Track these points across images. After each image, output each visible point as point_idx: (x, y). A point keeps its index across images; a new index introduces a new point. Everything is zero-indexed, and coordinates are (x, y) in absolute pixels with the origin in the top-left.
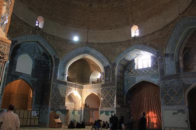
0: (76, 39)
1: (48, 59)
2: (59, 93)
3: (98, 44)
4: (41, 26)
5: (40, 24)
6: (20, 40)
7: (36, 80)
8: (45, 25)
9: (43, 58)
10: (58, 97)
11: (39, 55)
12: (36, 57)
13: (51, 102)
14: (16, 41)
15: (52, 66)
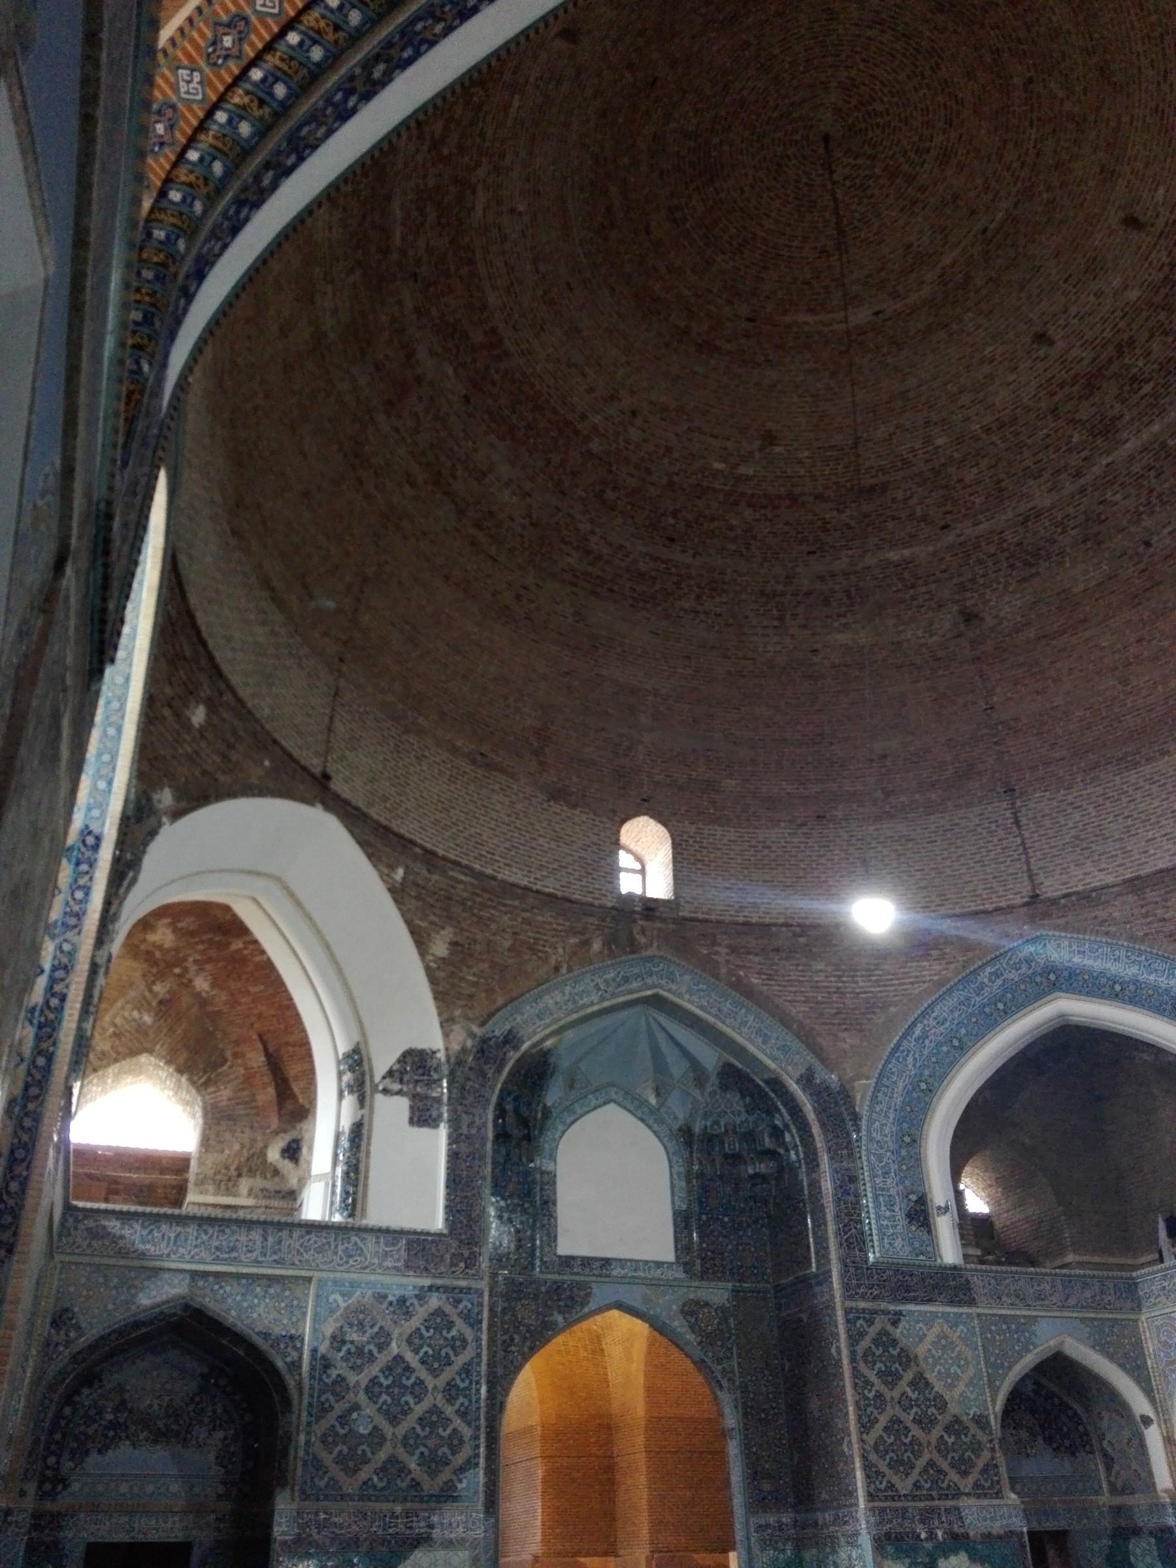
0: (873, 915)
1: (771, 1111)
2: (920, 1382)
3: (1135, 885)
4: (658, 882)
5: (646, 861)
6: (539, 1021)
7: (718, 1294)
8: (684, 860)
9: (734, 1110)
10: (926, 1423)
11: (696, 1093)
12: (678, 1110)
13: (867, 1466)
14: (511, 1039)
15: (813, 1162)
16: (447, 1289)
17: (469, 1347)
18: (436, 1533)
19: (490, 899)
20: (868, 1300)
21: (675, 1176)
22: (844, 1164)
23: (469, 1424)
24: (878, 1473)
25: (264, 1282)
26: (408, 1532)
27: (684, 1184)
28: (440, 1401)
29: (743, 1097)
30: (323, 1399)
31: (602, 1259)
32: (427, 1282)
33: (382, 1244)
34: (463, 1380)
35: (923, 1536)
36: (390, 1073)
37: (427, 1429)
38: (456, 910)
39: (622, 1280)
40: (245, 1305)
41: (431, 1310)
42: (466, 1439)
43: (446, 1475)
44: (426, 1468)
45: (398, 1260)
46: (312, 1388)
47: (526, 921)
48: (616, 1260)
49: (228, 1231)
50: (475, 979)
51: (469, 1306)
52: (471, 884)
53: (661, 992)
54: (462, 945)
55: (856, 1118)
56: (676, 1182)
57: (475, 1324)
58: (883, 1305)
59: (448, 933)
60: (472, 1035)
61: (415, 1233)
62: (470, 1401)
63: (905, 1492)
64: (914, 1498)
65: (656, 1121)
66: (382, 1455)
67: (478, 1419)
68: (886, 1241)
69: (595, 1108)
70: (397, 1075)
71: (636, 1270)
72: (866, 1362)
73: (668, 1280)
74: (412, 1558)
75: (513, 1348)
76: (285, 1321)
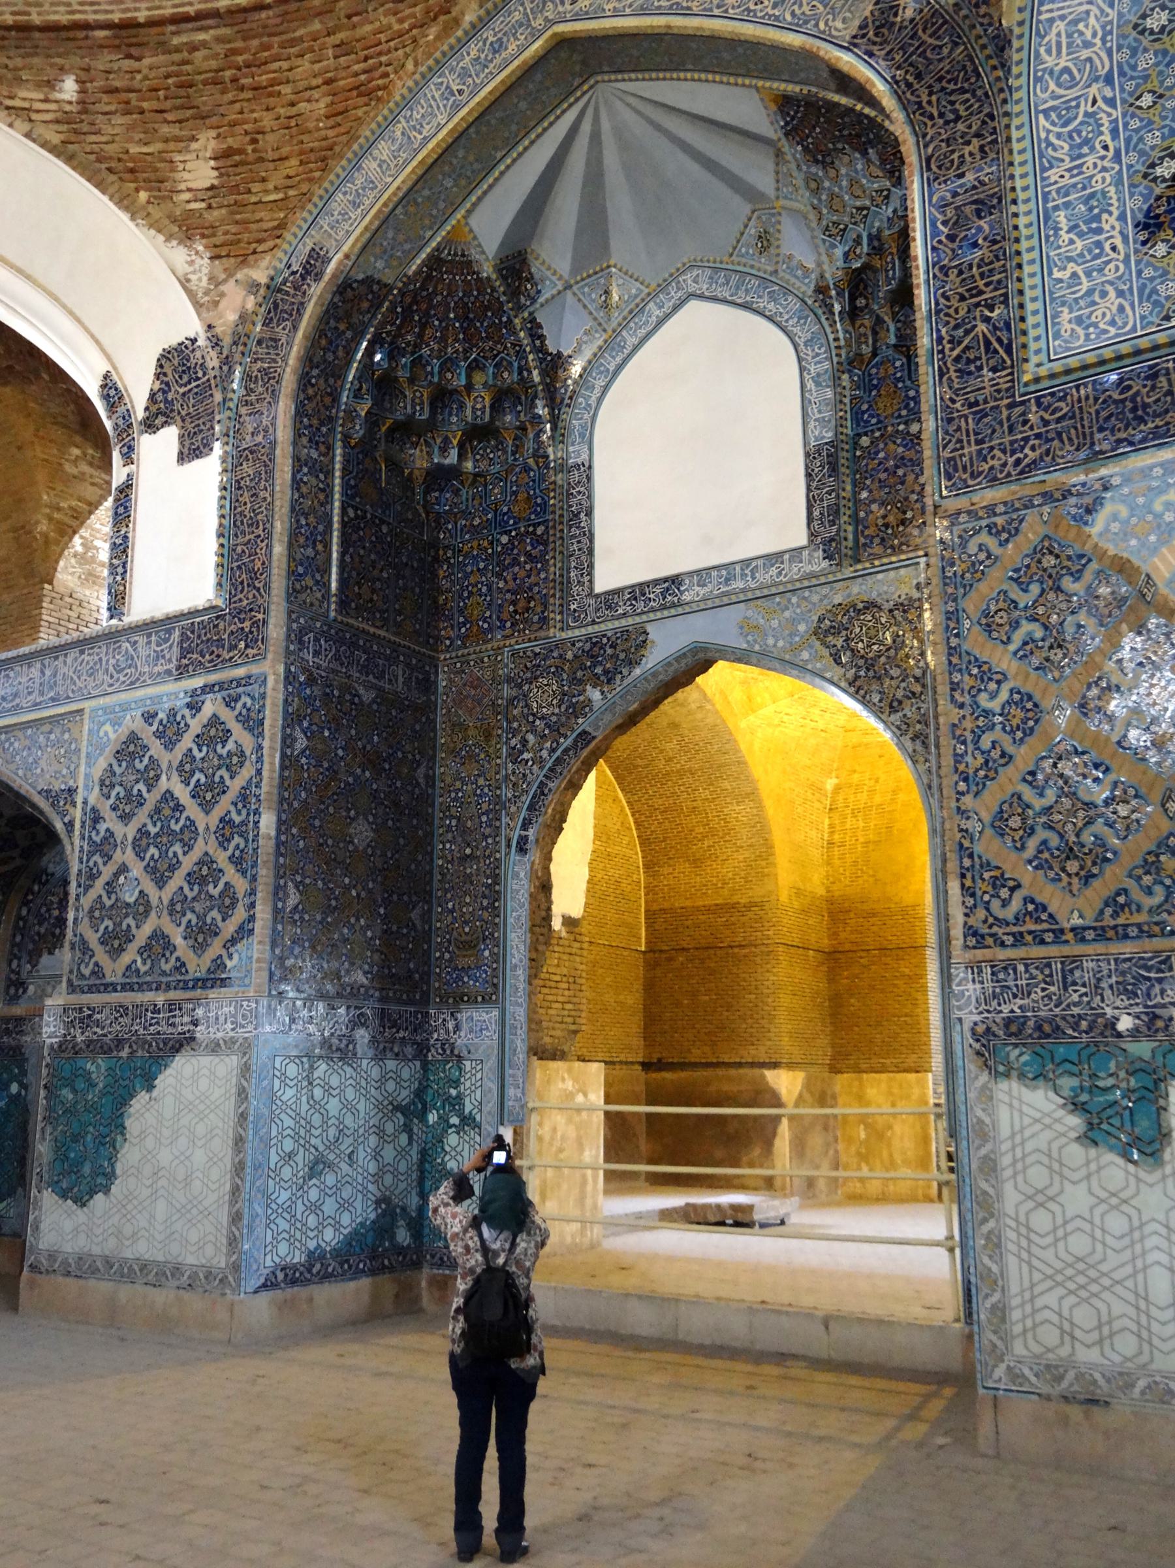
16: (221, 686)
17: (247, 763)
18: (200, 1032)
19: (266, 47)
20: (1008, 480)
21: (810, 385)
22: (970, 177)
23: (244, 873)
24: (998, 882)
25: (46, 728)
26: (171, 1030)
27: (829, 393)
28: (212, 848)
29: (864, 153)
30: (91, 864)
31: (665, 580)
32: (198, 682)
33: (153, 645)
34: (239, 813)
35: (1125, 1023)
36: (152, 397)
37: (196, 887)
38: (206, 99)
39: (708, 606)
40: (31, 760)
41: (205, 721)
42: (240, 896)
43: (216, 948)
44: (191, 942)
45: (170, 661)
46: (82, 850)
47: (343, 49)
48: (690, 574)
49: (12, 674)
50: (281, 196)
51: (249, 702)
52: (219, 40)
53: (560, 28)
54: (241, 151)
55: (1001, 43)
56: (813, 396)
57: (252, 723)
58: (1056, 478)
59: (207, 142)
60: (253, 287)
61: (182, 616)
62: (247, 841)
63: (1076, 921)
64: (1102, 934)
65: (772, 297)
66: (147, 929)
67: (255, 865)
68: (1066, 315)
69: (661, 322)
70: (160, 397)
71: (727, 580)
72: (988, 629)
73: (792, 581)
74: (174, 1065)
75: (526, 756)
76: (64, 772)
